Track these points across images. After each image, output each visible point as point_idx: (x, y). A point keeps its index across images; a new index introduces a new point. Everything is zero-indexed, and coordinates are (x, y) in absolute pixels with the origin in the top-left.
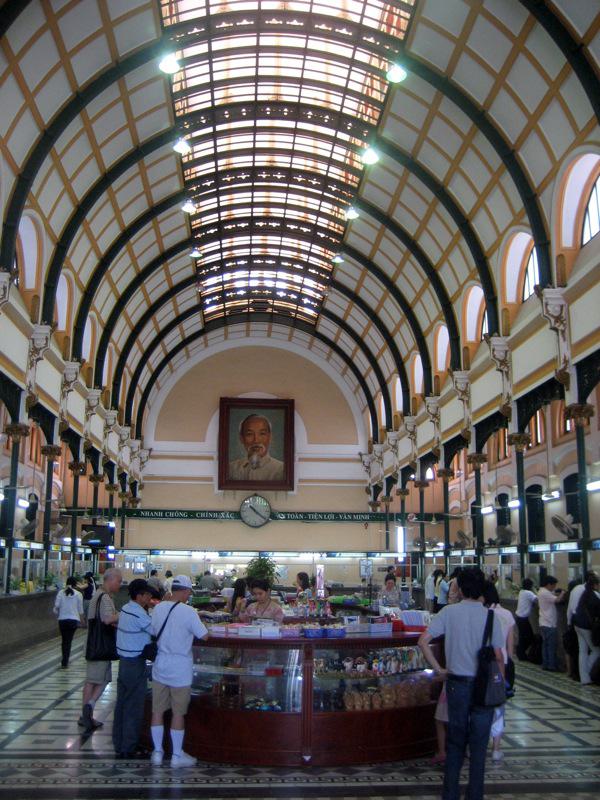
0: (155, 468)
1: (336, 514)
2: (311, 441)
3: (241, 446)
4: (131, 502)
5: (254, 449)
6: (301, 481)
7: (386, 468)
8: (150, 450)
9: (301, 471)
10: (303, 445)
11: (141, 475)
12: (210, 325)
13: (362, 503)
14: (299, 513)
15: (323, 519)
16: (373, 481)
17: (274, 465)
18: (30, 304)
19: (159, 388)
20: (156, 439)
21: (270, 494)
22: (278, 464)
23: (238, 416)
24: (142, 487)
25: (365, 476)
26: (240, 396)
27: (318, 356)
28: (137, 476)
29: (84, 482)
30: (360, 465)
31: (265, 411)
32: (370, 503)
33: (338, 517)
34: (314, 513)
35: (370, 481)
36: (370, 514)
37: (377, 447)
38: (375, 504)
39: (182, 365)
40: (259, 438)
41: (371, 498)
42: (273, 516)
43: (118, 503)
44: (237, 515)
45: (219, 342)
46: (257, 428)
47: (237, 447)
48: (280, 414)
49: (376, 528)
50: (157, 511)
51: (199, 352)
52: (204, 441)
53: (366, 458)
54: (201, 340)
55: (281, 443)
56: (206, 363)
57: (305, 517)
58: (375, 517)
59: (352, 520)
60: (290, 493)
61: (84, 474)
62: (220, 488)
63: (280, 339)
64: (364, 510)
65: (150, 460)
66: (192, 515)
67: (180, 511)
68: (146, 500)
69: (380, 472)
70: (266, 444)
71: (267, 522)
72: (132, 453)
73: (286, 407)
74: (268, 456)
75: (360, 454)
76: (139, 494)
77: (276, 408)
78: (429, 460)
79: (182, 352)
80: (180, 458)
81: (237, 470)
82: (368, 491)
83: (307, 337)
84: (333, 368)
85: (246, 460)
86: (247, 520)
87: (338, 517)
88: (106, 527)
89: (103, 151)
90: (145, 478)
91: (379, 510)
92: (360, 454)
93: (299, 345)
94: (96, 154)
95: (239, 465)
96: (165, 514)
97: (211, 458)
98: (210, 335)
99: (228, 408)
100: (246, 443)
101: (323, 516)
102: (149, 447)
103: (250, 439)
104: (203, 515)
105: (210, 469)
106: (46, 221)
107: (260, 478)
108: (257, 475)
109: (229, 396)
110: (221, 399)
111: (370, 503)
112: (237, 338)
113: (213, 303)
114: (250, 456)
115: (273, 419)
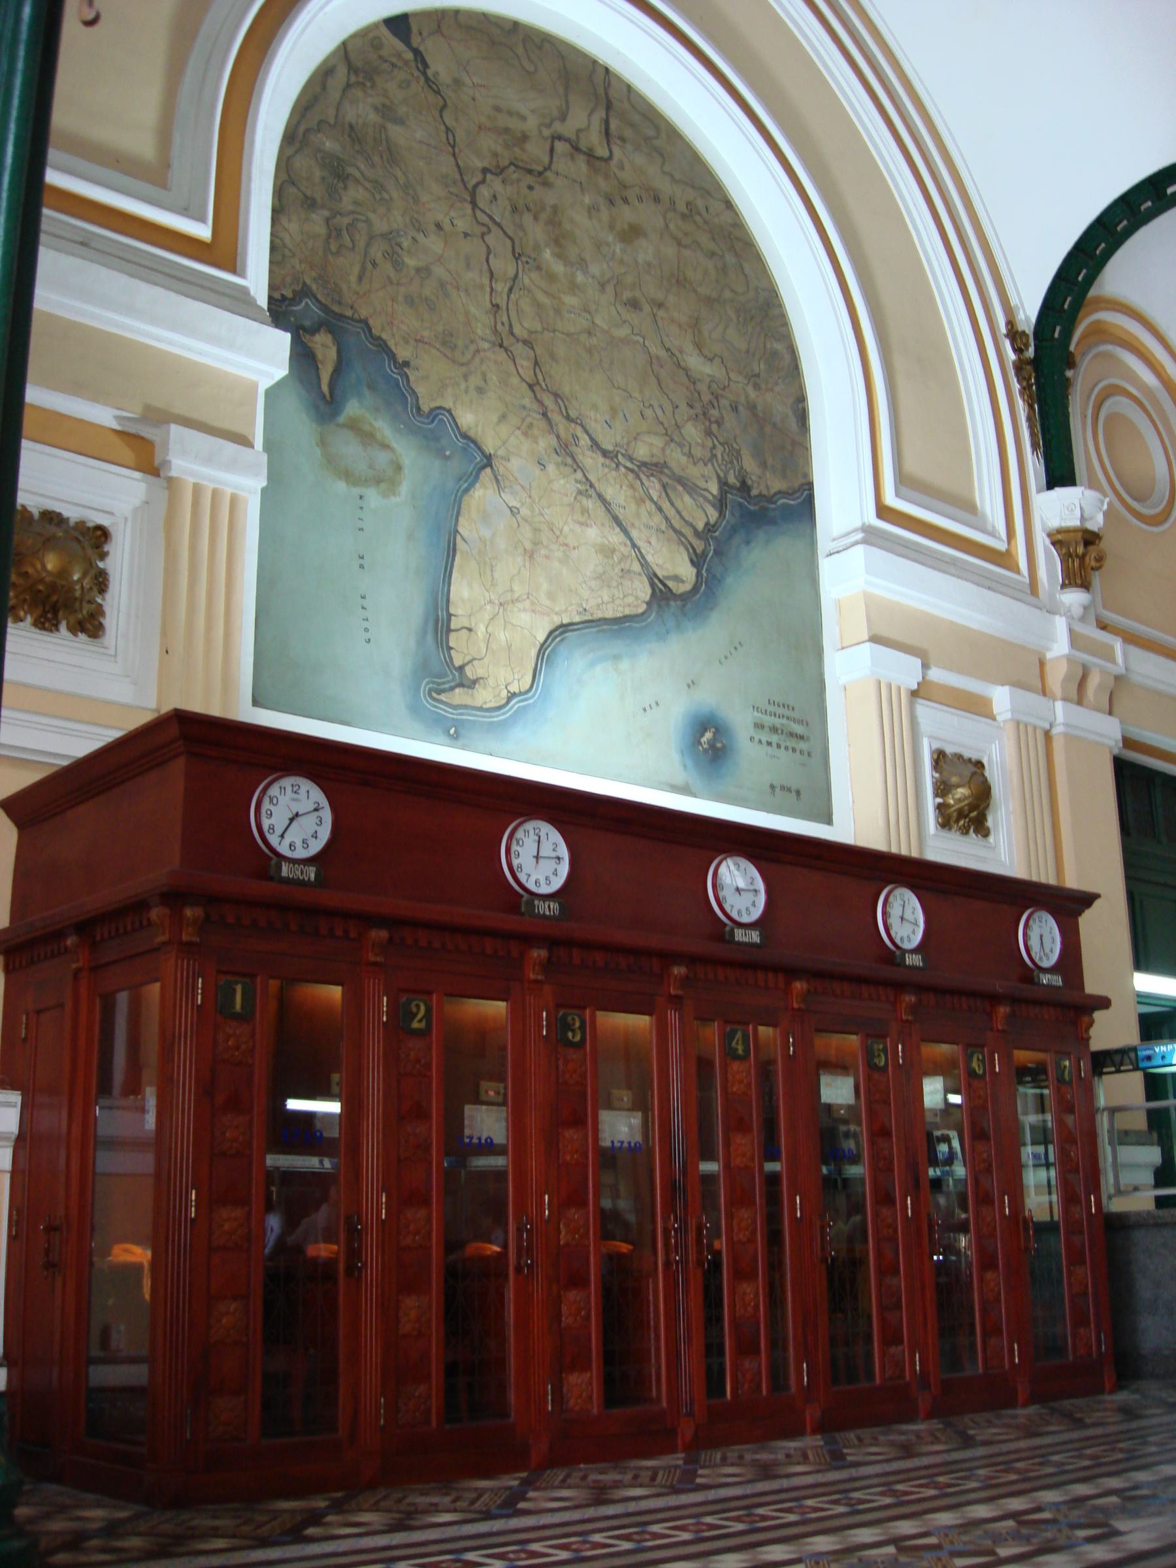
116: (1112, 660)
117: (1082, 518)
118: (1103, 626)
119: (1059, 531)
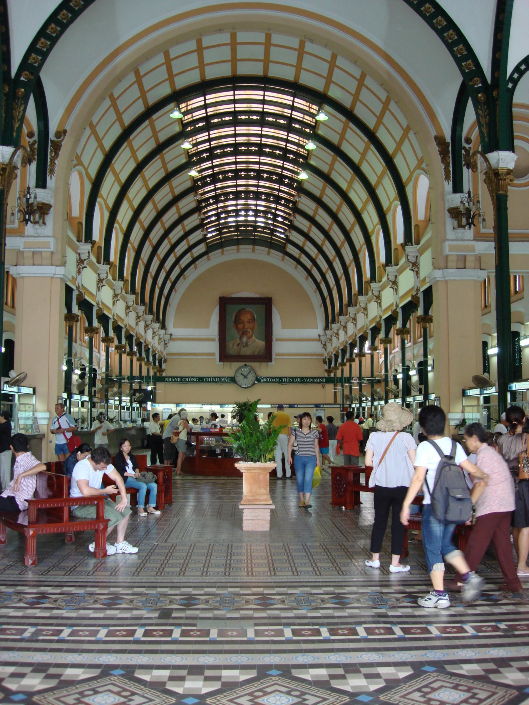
1: (302, 378)
2: (284, 327)
5: (244, 333)
6: (277, 355)
8: (171, 335)
9: (278, 348)
11: (165, 353)
13: (320, 371)
14: (275, 378)
15: (293, 382)
16: (328, 354)
18: (76, 230)
20: (174, 328)
22: (261, 344)
23: (232, 310)
24: (165, 361)
25: (323, 351)
26: (233, 296)
27: (288, 266)
28: (162, 353)
29: (126, 358)
30: (319, 343)
32: (326, 371)
33: (303, 380)
34: (286, 378)
35: (326, 354)
36: (326, 378)
38: (329, 371)
39: (192, 274)
40: (247, 325)
41: (326, 367)
44: (233, 380)
45: (217, 258)
46: (246, 318)
47: (232, 332)
48: (262, 308)
49: (330, 387)
50: (177, 377)
51: (203, 265)
52: (208, 327)
53: (322, 338)
54: (205, 257)
56: (209, 271)
57: (281, 380)
58: (329, 380)
59: (314, 382)
61: (125, 352)
62: (220, 361)
63: (261, 254)
64: (322, 375)
65: (171, 342)
66: (201, 380)
67: (192, 377)
68: (169, 370)
69: (331, 349)
70: (252, 330)
71: (254, 384)
73: (266, 303)
74: (254, 337)
75: (319, 336)
76: (164, 366)
77: (258, 304)
79: (193, 266)
81: (232, 349)
82: (325, 362)
83: (281, 255)
84: (300, 275)
85: (238, 341)
86: (239, 383)
87: (303, 380)
89: (124, 116)
90: (168, 354)
91: (332, 375)
92: (319, 336)
93: (274, 258)
94: (120, 118)
95: (233, 345)
96: (183, 380)
97: (213, 340)
98: (210, 254)
100: (237, 328)
101: (293, 380)
102: (170, 333)
103: (240, 326)
104: (208, 380)
105: (214, 347)
106: (86, 170)
107: (248, 354)
109: (225, 296)
111: (326, 371)
112: (230, 254)
114: (241, 338)
115: (257, 311)
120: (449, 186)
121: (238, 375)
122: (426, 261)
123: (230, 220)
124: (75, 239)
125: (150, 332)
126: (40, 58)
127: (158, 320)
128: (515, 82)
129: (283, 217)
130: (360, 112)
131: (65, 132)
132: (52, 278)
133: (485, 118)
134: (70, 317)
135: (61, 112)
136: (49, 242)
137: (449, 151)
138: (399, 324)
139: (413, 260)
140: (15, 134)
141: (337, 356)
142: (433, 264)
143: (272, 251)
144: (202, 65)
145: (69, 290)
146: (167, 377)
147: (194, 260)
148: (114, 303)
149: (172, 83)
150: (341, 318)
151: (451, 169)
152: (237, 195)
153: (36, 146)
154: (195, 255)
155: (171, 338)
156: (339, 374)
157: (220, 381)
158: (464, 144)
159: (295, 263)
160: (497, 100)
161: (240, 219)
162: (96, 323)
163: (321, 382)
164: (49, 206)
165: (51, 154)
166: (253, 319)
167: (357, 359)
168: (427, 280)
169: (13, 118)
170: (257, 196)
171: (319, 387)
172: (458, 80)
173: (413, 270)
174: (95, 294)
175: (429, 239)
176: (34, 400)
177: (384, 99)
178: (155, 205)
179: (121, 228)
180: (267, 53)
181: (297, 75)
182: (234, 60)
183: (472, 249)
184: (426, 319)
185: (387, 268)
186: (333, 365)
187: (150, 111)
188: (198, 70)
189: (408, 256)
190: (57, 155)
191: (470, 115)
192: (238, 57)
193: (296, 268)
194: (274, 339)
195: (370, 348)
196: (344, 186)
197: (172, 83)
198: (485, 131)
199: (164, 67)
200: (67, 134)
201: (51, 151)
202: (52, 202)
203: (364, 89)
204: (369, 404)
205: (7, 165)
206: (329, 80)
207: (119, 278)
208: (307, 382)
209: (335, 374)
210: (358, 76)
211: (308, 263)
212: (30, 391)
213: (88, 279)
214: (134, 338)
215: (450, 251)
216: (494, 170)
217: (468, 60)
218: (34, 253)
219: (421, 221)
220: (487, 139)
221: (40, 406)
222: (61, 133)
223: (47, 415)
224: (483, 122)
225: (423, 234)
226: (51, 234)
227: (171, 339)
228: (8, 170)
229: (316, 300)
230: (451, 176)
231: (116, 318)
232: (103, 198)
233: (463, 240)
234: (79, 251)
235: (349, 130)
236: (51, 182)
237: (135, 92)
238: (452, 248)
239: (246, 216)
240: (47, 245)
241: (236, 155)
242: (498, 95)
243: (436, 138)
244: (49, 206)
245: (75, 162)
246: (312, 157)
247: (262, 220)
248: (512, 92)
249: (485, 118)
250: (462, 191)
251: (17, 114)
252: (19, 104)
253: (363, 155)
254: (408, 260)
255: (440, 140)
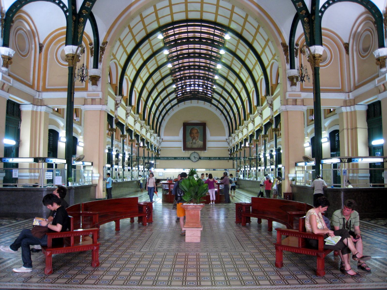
0: (164, 144)
1: (219, 158)
2: (211, 136)
3: (190, 137)
4: (157, 155)
5: (194, 138)
6: (208, 148)
7: (233, 143)
8: (162, 139)
9: (209, 145)
10: (209, 137)
11: (160, 147)
12: (179, 101)
13: (227, 154)
14: (208, 157)
16: (230, 147)
17: (200, 143)
19: (164, 120)
21: (199, 152)
22: (201, 143)
23: (189, 128)
24: (160, 150)
25: (228, 146)
27: (213, 109)
28: (158, 147)
30: (227, 142)
31: (197, 126)
33: (220, 158)
35: (229, 147)
37: (230, 138)
38: (231, 155)
39: (171, 113)
40: (195, 135)
41: (229, 153)
42: (200, 158)
43: (154, 156)
44: (189, 158)
45: (182, 105)
46: (195, 131)
47: (189, 138)
48: (202, 127)
49: (231, 161)
51: (176, 109)
54: (177, 105)
55: (202, 136)
57: (210, 158)
58: (231, 158)
59: (224, 159)
60: (205, 151)
62: (184, 150)
63: (201, 104)
64: (228, 157)
65: (163, 142)
66: (175, 158)
68: (162, 154)
69: (231, 145)
70: (198, 137)
71: (198, 160)
72: (158, 141)
73: (203, 125)
74: (198, 140)
75: (226, 139)
76: (159, 153)
78: (246, 140)
79: (171, 109)
80: (173, 142)
81: (189, 145)
82: (229, 150)
83: (210, 104)
84: (218, 113)
85: (191, 142)
86: (192, 160)
87: (220, 158)
88: (151, 163)
90: (161, 148)
91: (232, 156)
92: (226, 139)
93: (207, 105)
96: (167, 158)
97: (181, 141)
98: (179, 104)
99: (186, 126)
101: (215, 158)
103: (192, 135)
105: (181, 144)
108: (195, 146)
109: (186, 122)
110: (183, 123)
113: (180, 94)
114: (192, 140)
115: (199, 129)
116: (10, 82)
117: (9, 54)
118: (9, 75)
119: (4, 55)
120: (288, 66)
121: (191, 156)
122: (277, 104)
123: (188, 88)
124: (114, 94)
125: (153, 138)
126: (91, 4)
127: (156, 132)
128: (323, 13)
129: (210, 87)
130: (245, 35)
131: (107, 43)
132: (100, 111)
133: (308, 30)
134: (111, 130)
135: (105, 33)
136: (99, 94)
137: (288, 50)
138: (263, 133)
139: (270, 102)
140: (79, 40)
141: (234, 148)
142: (281, 103)
143: (206, 103)
144: (172, 14)
145: (110, 118)
146: (161, 157)
147: (172, 107)
148: (135, 124)
149: (158, 23)
150: (236, 131)
151: (289, 58)
152: (190, 77)
153: (93, 49)
154: (173, 105)
155: (163, 140)
156: (235, 156)
157: (184, 159)
158: (295, 47)
159: (216, 108)
160: (314, 21)
161: (192, 88)
162: (125, 133)
163: (227, 159)
164: (99, 77)
165: (100, 53)
166: (198, 132)
167: (243, 150)
168: (278, 111)
169: (78, 32)
170: (199, 78)
171: (227, 161)
172: (295, 11)
173: (270, 108)
174: (125, 120)
175: (279, 92)
176: (92, 168)
177: (256, 27)
178: (153, 81)
179: (137, 91)
180: (202, 7)
181: (216, 18)
182: (187, 11)
183: (300, 96)
184: (277, 129)
185: (258, 107)
186: (232, 152)
187: (148, 36)
188: (170, 16)
189: (268, 101)
190: (103, 53)
191: (300, 29)
192: (189, 9)
193: (216, 110)
194: (207, 141)
195: (249, 144)
196: (237, 71)
197: (158, 23)
198: (308, 36)
199: (154, 14)
200: (108, 44)
201: (100, 51)
202: (101, 75)
203: (247, 23)
204: (249, 169)
205: (74, 55)
206: (231, 19)
207: (137, 113)
208: (221, 159)
209: (233, 156)
210: (244, 16)
211: (221, 108)
212: (90, 164)
213: (121, 113)
214: (145, 140)
215: (289, 97)
216: (313, 55)
217: (299, 2)
218: (92, 99)
219: (274, 85)
220: (309, 40)
221: (95, 171)
222: (105, 43)
223: (98, 175)
224: (307, 32)
225: (275, 91)
226: (100, 90)
227: (162, 141)
228: (75, 57)
229: (225, 124)
230: (289, 61)
231: (135, 131)
232: (127, 76)
233: (295, 91)
234: (116, 100)
235: (240, 44)
236: (100, 66)
237: (141, 26)
238: (290, 95)
239: (194, 87)
240: (98, 95)
241: (189, 58)
242: (315, 18)
243: (282, 44)
244: (99, 77)
245: (112, 57)
246: (223, 58)
247: (201, 89)
248: (321, 17)
249: (308, 30)
250: (294, 68)
251: (80, 30)
252: (81, 26)
253: (246, 56)
254: (268, 102)
255: (284, 45)
